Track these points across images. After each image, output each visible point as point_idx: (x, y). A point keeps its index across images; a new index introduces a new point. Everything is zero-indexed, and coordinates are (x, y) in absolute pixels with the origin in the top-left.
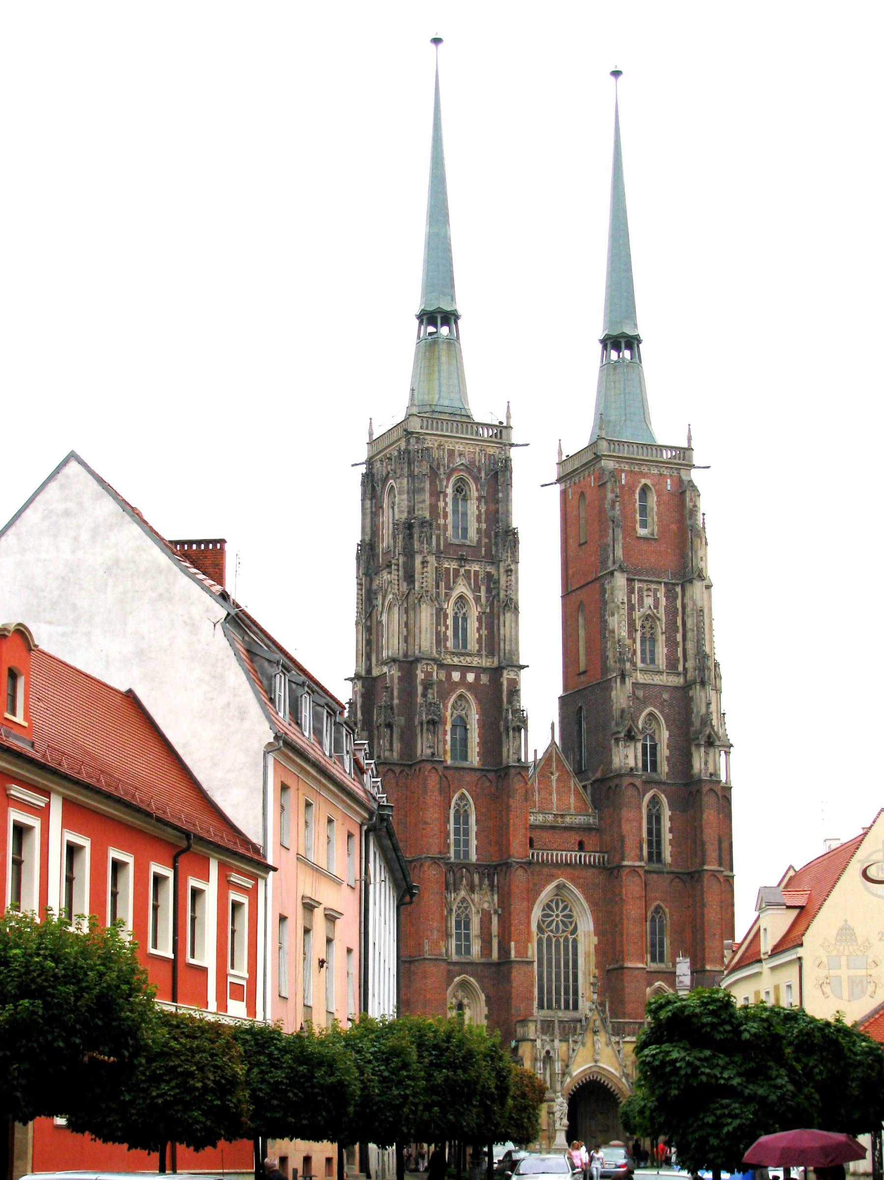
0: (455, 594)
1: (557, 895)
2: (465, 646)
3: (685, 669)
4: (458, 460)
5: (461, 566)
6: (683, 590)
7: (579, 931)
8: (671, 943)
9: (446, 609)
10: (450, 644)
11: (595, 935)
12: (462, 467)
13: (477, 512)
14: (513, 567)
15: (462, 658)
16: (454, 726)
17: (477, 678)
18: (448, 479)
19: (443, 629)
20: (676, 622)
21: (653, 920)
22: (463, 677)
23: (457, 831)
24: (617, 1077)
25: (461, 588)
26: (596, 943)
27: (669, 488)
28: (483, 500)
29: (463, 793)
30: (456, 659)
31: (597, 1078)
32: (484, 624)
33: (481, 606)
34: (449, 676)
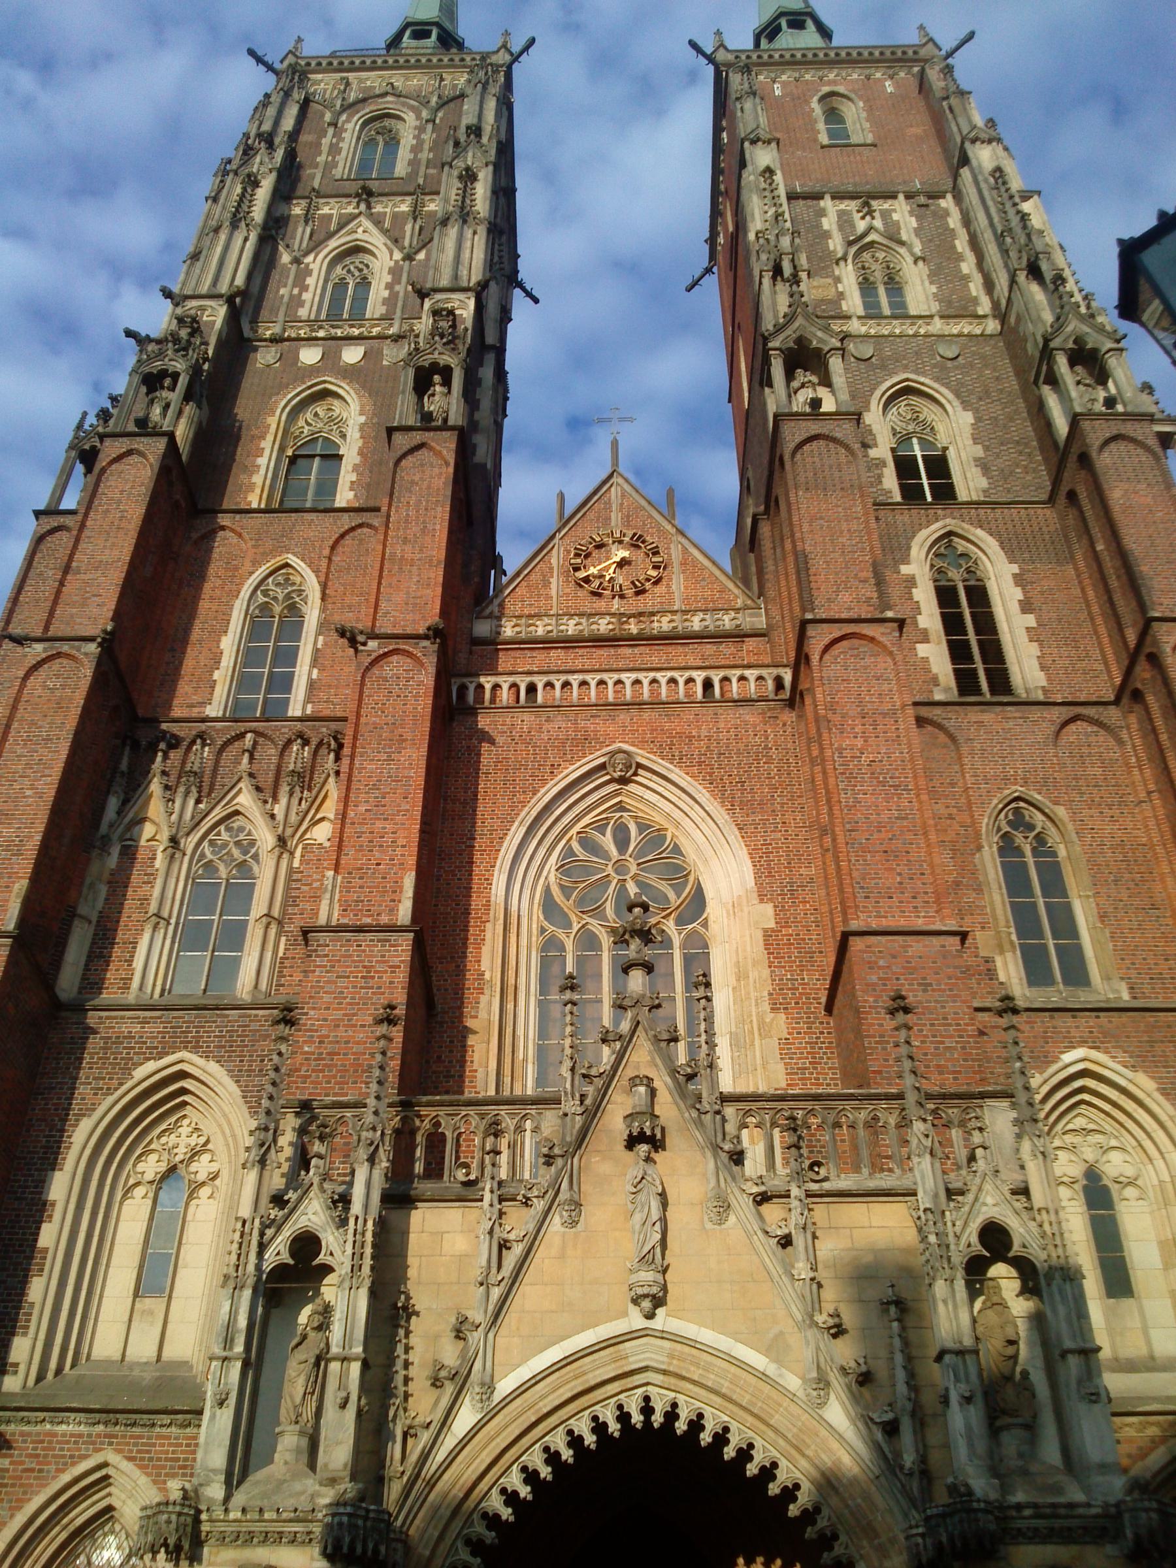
1: (620, 807)
3: (996, 305)
5: (358, 206)
6: (958, 198)
7: (714, 910)
8: (1103, 917)
9: (308, 265)
11: (762, 898)
19: (296, 291)
21: (1007, 847)
24: (792, 1397)
26: (772, 924)
28: (430, 126)
29: (287, 565)
31: (672, 1415)
33: (402, 249)
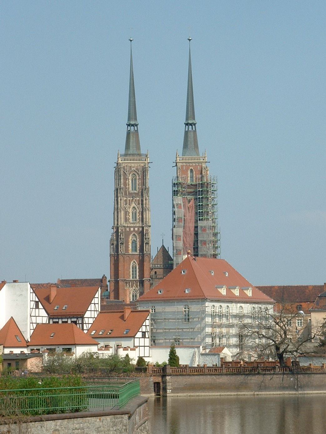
0: (132, 207)
2: (136, 220)
4: (132, 169)
10: (131, 220)
12: (133, 171)
13: (138, 183)
14: (147, 198)
15: (134, 224)
16: (132, 243)
17: (138, 229)
18: (129, 175)
19: (128, 217)
22: (134, 229)
23: (133, 271)
25: (133, 205)
27: (199, 169)
30: (132, 224)
34: (130, 229)
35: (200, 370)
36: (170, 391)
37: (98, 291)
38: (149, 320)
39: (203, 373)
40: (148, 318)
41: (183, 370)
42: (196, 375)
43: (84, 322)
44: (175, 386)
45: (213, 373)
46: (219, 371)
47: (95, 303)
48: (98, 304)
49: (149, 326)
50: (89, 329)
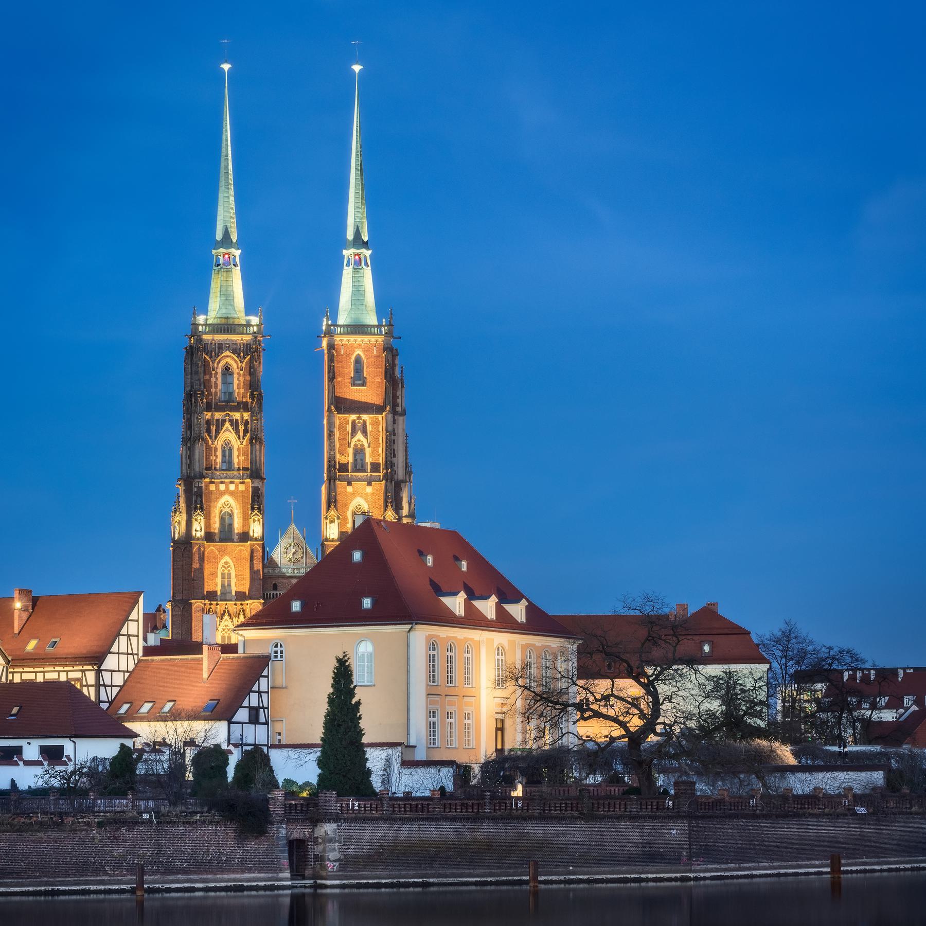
17: (237, 487)
19: (214, 458)
20: (379, 440)
32: (241, 453)
35: (420, 807)
36: (337, 864)
37: (138, 602)
38: (267, 677)
39: (430, 815)
40: (265, 673)
41: (374, 806)
42: (409, 820)
43: (101, 683)
44: (351, 851)
45: (459, 814)
46: (475, 809)
47: (129, 634)
48: (137, 636)
49: (268, 692)
50: (113, 701)
